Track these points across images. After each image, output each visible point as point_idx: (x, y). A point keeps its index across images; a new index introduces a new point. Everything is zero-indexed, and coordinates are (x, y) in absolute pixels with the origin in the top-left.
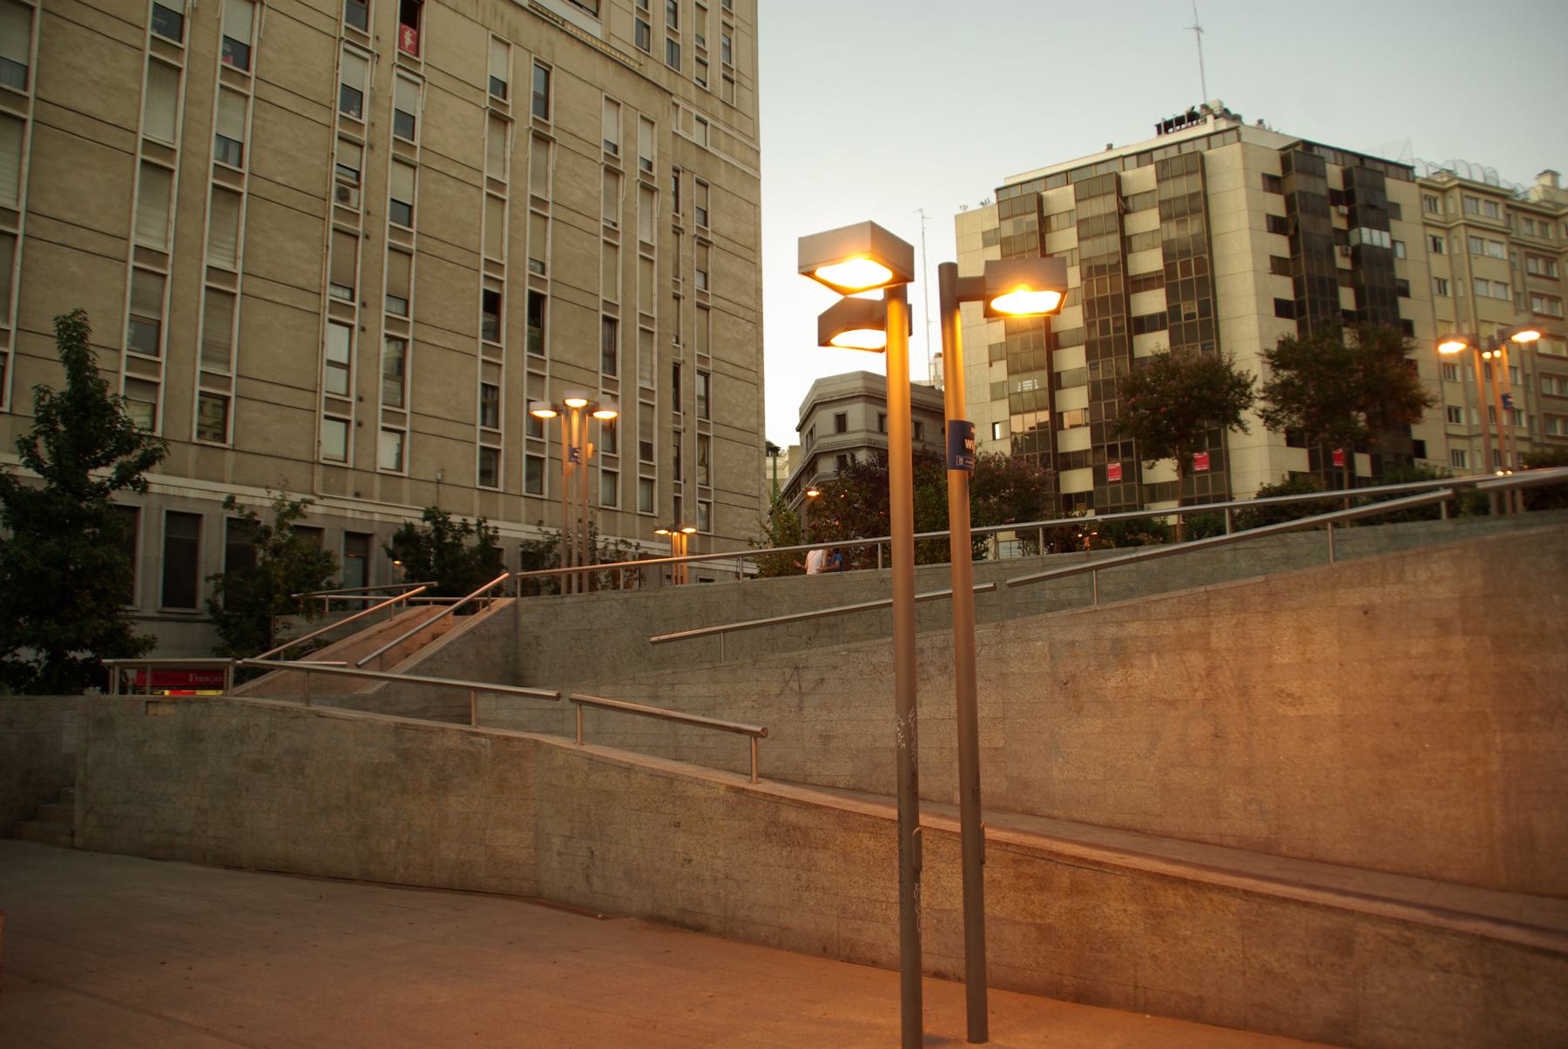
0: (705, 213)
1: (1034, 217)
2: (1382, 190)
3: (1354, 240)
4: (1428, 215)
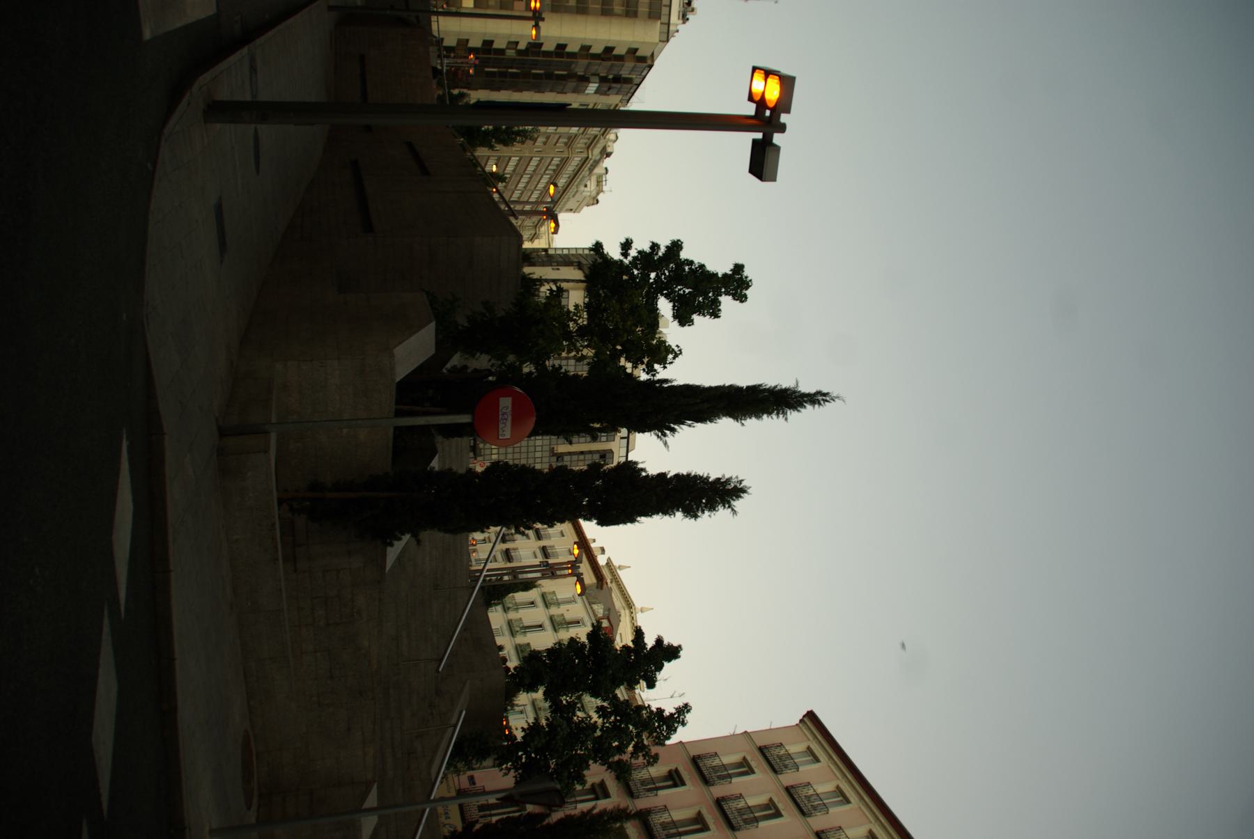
3: (592, 79)
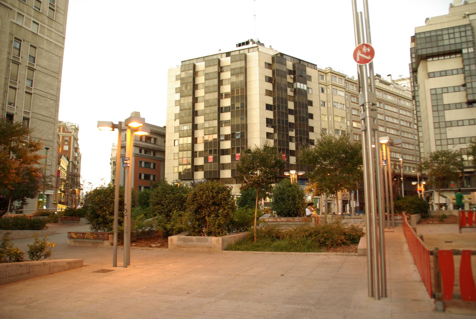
0: (34, 58)
1: (192, 71)
2: (305, 71)
3: (295, 87)
4: (320, 81)
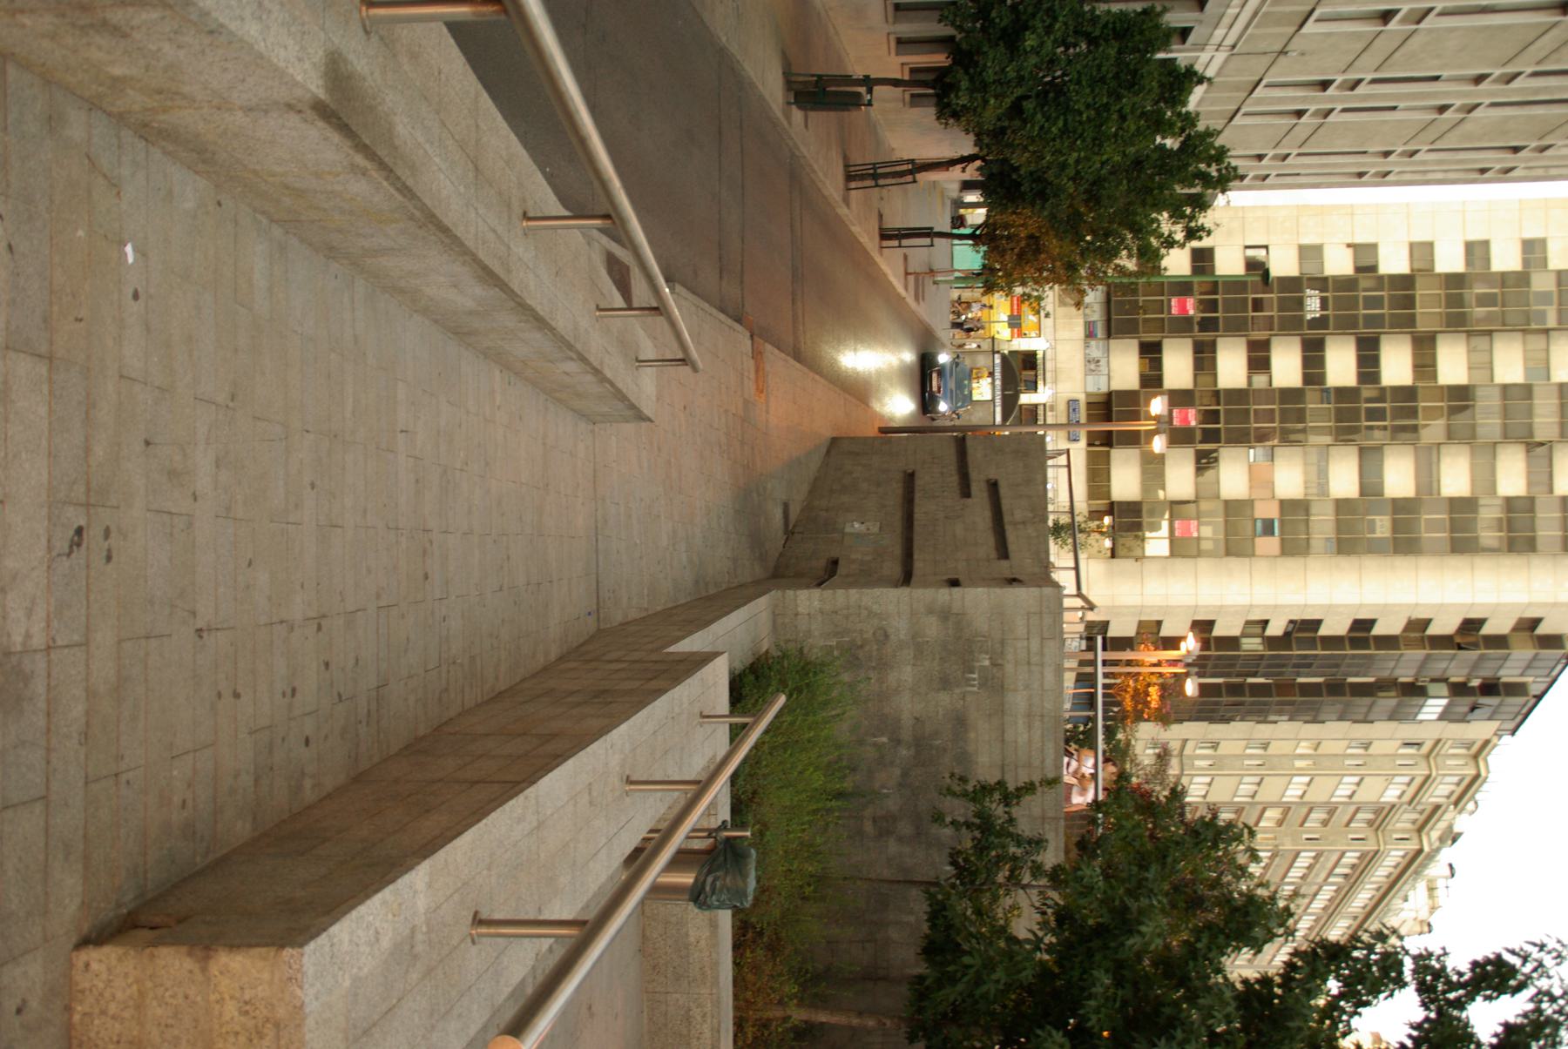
3: (1433, 688)
